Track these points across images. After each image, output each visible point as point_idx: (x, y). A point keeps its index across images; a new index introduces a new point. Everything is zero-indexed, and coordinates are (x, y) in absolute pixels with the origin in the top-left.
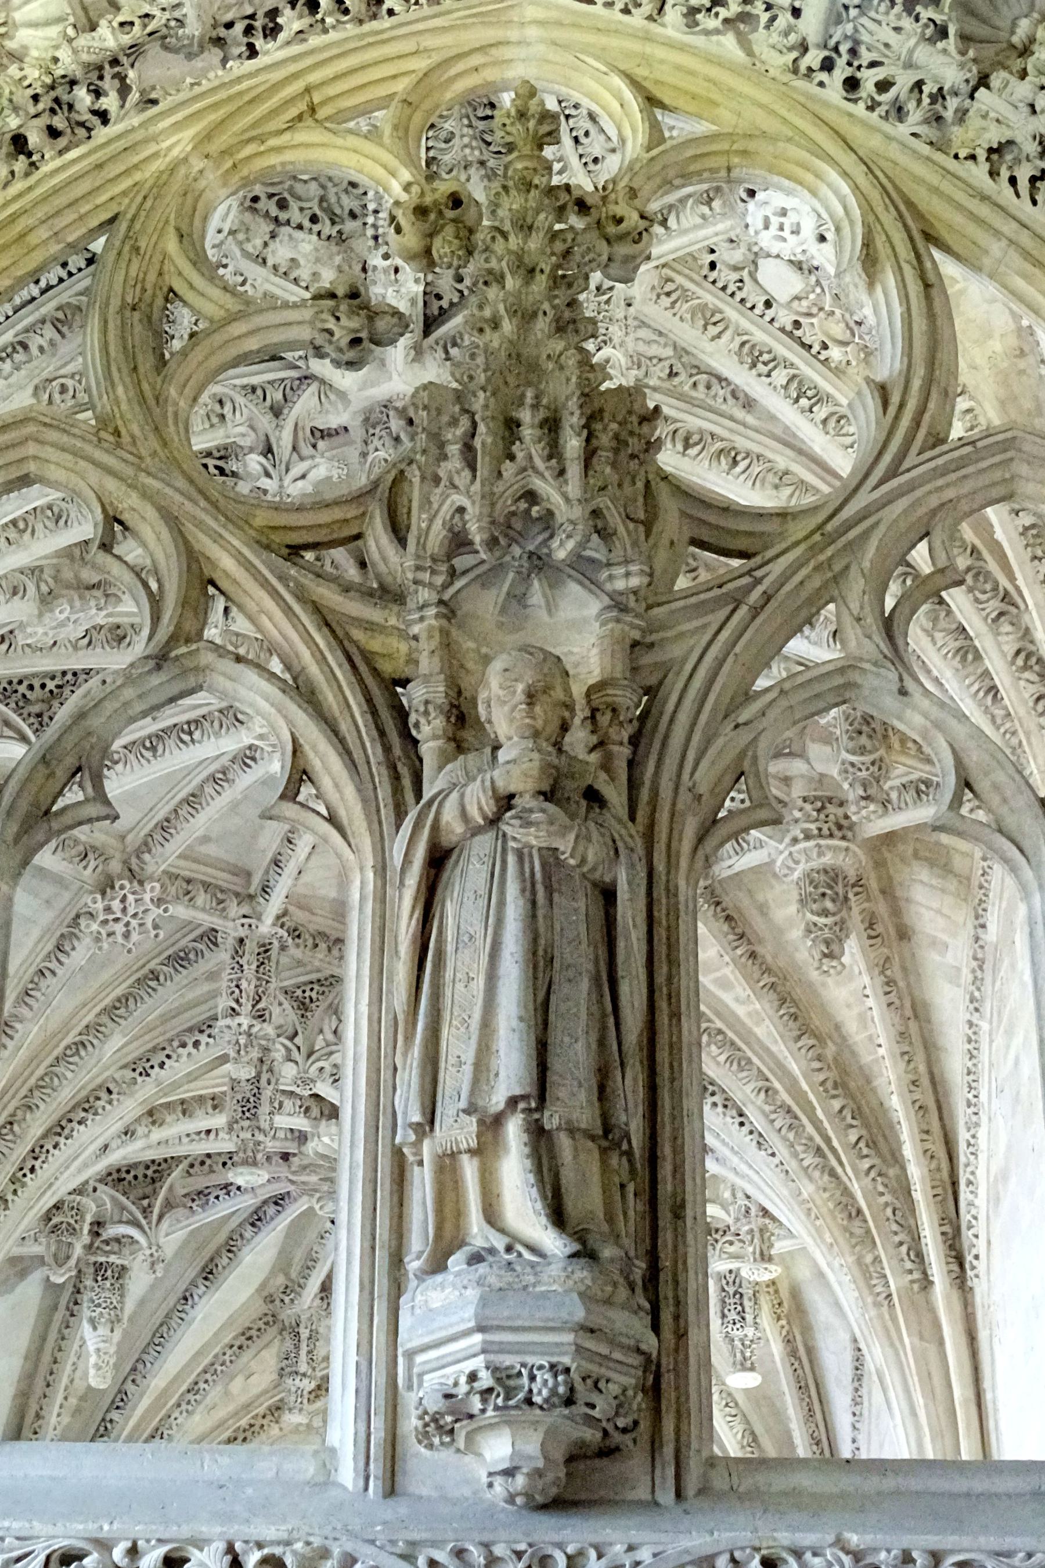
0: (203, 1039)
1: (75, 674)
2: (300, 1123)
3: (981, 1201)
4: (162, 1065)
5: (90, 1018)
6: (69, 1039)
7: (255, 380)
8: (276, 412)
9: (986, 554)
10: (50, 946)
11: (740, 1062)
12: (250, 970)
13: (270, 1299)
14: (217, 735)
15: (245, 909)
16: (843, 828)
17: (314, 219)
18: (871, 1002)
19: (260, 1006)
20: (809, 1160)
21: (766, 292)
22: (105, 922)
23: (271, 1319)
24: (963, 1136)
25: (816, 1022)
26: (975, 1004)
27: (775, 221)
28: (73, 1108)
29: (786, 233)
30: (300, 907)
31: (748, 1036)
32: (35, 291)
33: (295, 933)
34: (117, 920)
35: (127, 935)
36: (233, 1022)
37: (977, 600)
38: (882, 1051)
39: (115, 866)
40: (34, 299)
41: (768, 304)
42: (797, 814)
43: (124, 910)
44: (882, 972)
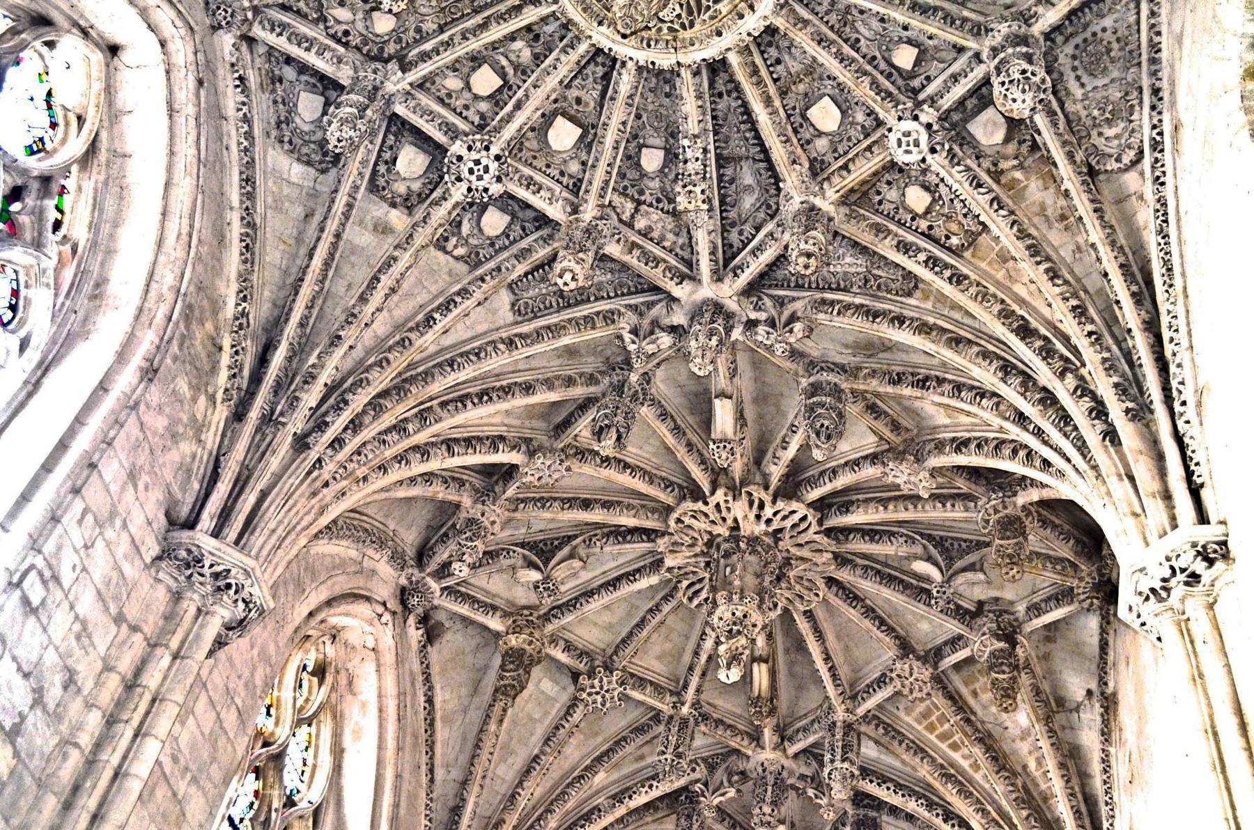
0: (655, 783)
4: (630, 797)
5: (588, 762)
6: (576, 774)
7: (632, 302)
8: (641, 315)
9: (1054, 340)
10: (562, 713)
11: (964, 793)
14: (648, 576)
15: (675, 699)
17: (659, 200)
19: (680, 750)
21: (911, 211)
22: (590, 694)
26: (1106, 734)
27: (904, 140)
28: (579, 819)
29: (911, 148)
30: (709, 704)
32: (507, 243)
33: (705, 717)
34: (597, 693)
35: (603, 705)
36: (662, 758)
37: (1049, 364)
40: (506, 248)
41: (913, 219)
43: (601, 688)
44: (1046, 724)
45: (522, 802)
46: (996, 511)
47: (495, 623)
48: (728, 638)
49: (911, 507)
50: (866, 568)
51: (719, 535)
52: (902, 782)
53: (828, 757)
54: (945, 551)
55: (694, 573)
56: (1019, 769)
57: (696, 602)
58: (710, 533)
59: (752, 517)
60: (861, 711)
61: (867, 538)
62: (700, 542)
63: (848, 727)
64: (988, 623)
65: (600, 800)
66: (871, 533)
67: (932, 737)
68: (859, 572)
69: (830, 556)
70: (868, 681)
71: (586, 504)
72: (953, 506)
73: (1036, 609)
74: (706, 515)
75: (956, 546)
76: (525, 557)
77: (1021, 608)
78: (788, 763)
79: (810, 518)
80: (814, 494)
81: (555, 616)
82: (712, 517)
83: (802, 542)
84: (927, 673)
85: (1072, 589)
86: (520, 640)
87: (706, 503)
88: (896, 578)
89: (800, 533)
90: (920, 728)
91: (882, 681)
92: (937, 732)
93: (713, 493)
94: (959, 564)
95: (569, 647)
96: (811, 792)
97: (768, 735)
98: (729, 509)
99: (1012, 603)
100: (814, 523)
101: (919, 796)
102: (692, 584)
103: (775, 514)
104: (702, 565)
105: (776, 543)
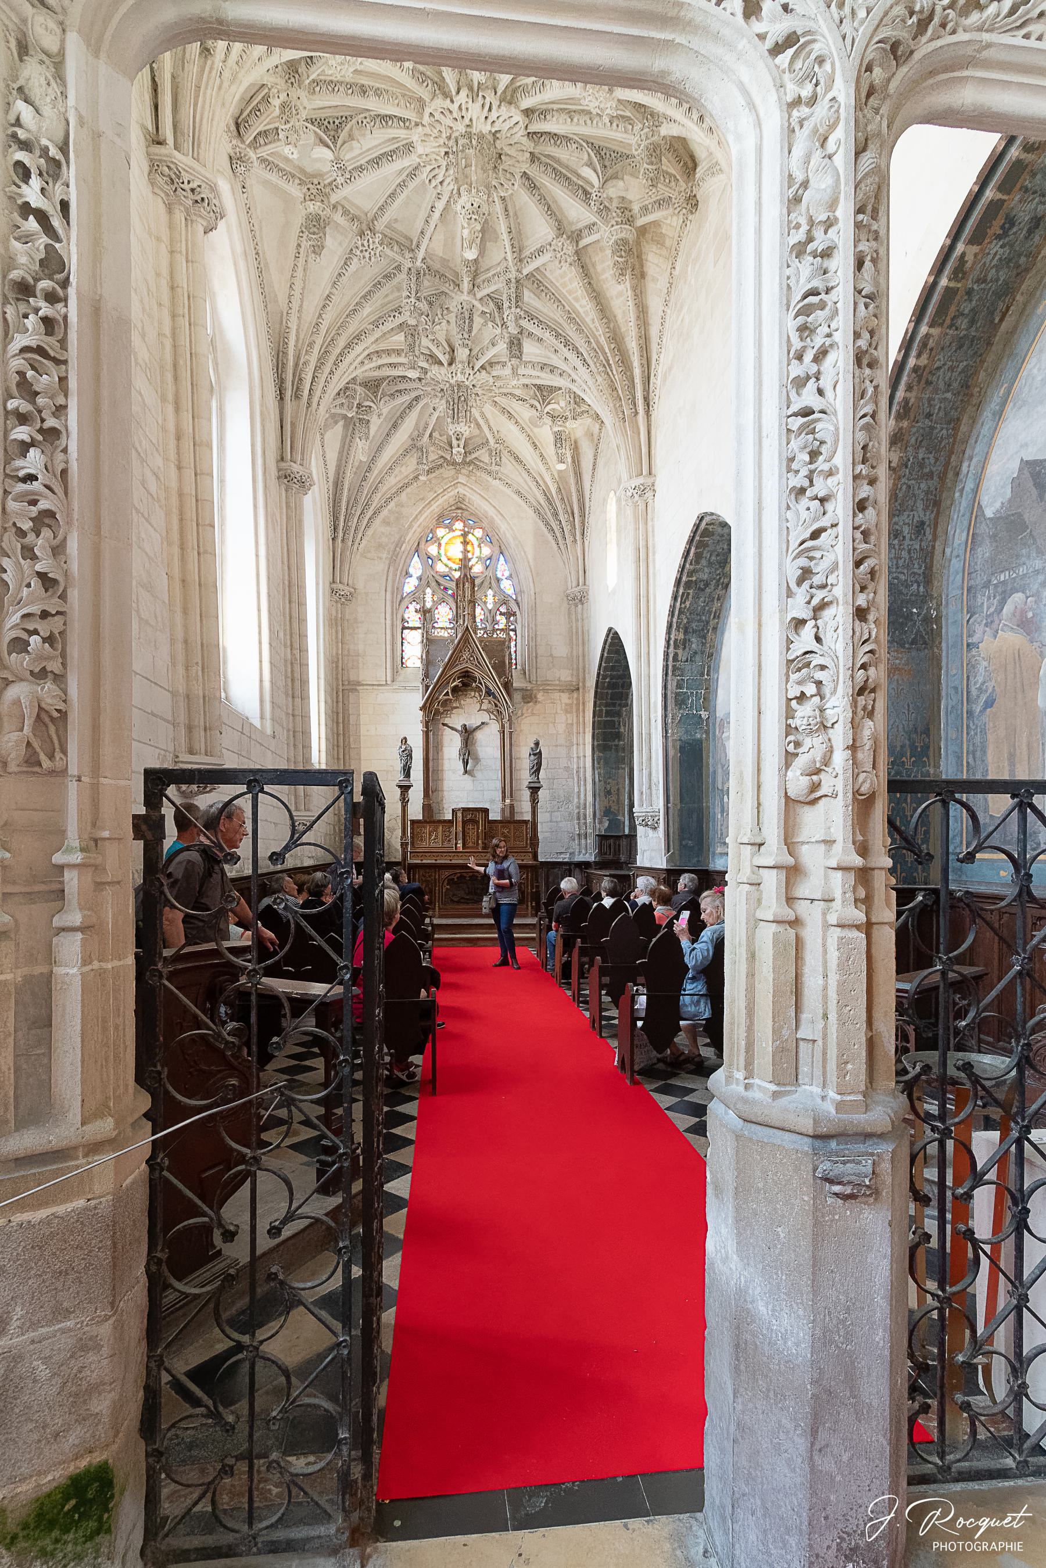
2: (425, 365)
3: (658, 382)
6: (351, 308)
12: (414, 280)
13: (413, 440)
15: (411, 255)
16: (630, 221)
18: (630, 303)
20: (601, 369)
22: (362, 251)
23: (414, 446)
24: (654, 357)
25: (608, 314)
31: (583, 321)
35: (370, 258)
38: (631, 324)
45: (323, 328)
46: (647, 138)
48: (469, 224)
53: (506, 305)
57: (434, 183)
58: (451, 128)
60: (525, 272)
61: (552, 141)
62: (444, 135)
64: (615, 216)
66: (554, 137)
70: (532, 250)
71: (363, 91)
73: (645, 210)
74: (451, 112)
76: (315, 132)
77: (636, 208)
79: (521, 123)
80: (527, 103)
82: (455, 115)
84: (570, 249)
86: (317, 208)
87: (452, 101)
88: (565, 176)
90: (558, 285)
91: (540, 251)
93: (458, 92)
94: (610, 172)
95: (346, 212)
96: (490, 324)
99: (631, 202)
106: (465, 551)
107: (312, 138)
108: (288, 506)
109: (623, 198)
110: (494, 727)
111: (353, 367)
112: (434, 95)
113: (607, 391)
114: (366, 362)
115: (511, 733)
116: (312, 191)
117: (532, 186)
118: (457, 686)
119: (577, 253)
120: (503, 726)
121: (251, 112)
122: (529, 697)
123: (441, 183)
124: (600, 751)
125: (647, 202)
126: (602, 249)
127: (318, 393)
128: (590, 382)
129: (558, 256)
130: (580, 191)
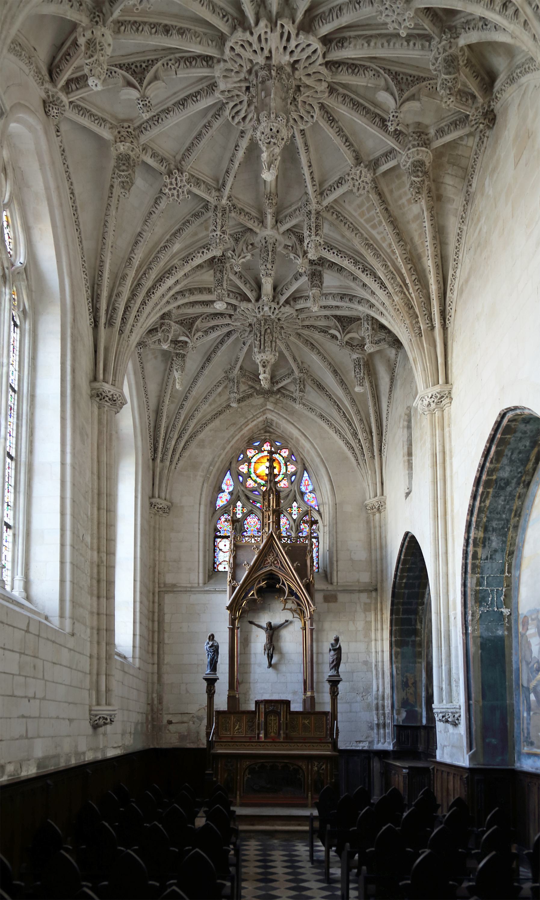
0: (205, 251)
1: (152, 61)
4: (192, 259)
5: (168, 237)
39: (172, 167)
42: (411, 138)
47: (106, 134)
49: (386, 44)
50: (345, 96)
51: (257, 63)
52: (340, 249)
54: (398, 83)
55: (238, 95)
56: (408, 240)
57: (237, 120)
58: (251, 61)
59: (281, 50)
60: (325, 203)
63: (318, 213)
65: (175, 262)
67: (362, 221)
68: (340, 99)
69: (326, 85)
72: (414, 44)
73: (441, 132)
75: (405, 80)
77: (432, 132)
78: (279, 238)
79: (319, 51)
81: (146, 129)
83: (311, 72)
84: (368, 176)
85: (467, 116)
87: (252, 34)
89: (310, 64)
92: (365, 218)
94: (406, 95)
95: (154, 155)
96: (292, 256)
97: (270, 220)
98: (266, 39)
100: (321, 56)
101: (351, 258)
102: (236, 105)
103: (297, 46)
104: (244, 89)
105: (293, 72)
106: (271, 468)
107: (121, 81)
108: (100, 422)
109: (419, 124)
110: (298, 625)
111: (165, 300)
112: (234, 29)
113: (404, 310)
114: (179, 297)
115: (312, 630)
116: (122, 133)
117: (331, 120)
118: (261, 587)
119: (374, 180)
120: (305, 623)
121: (61, 58)
122: (330, 598)
123: (244, 119)
124: (397, 646)
125: (442, 125)
126: (399, 177)
127: (131, 321)
128: (387, 303)
129: (357, 183)
130: (377, 119)
